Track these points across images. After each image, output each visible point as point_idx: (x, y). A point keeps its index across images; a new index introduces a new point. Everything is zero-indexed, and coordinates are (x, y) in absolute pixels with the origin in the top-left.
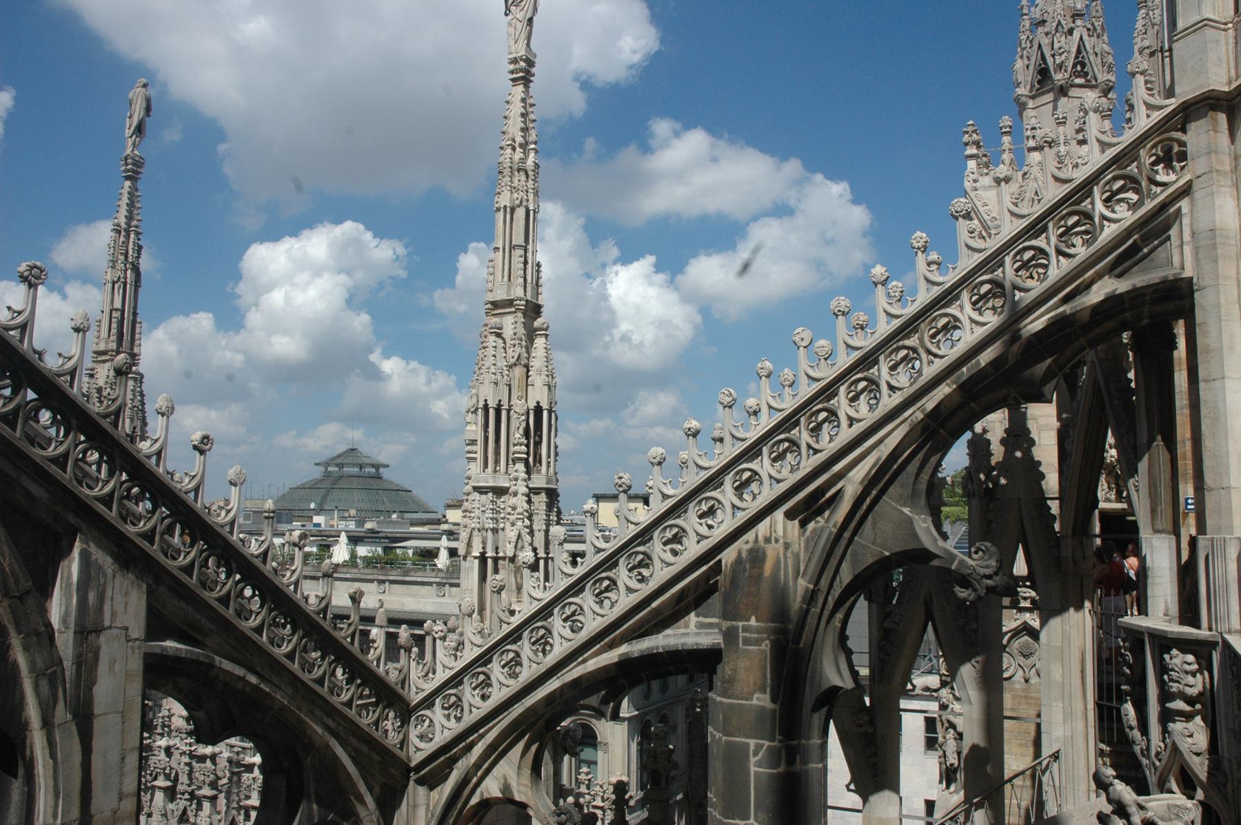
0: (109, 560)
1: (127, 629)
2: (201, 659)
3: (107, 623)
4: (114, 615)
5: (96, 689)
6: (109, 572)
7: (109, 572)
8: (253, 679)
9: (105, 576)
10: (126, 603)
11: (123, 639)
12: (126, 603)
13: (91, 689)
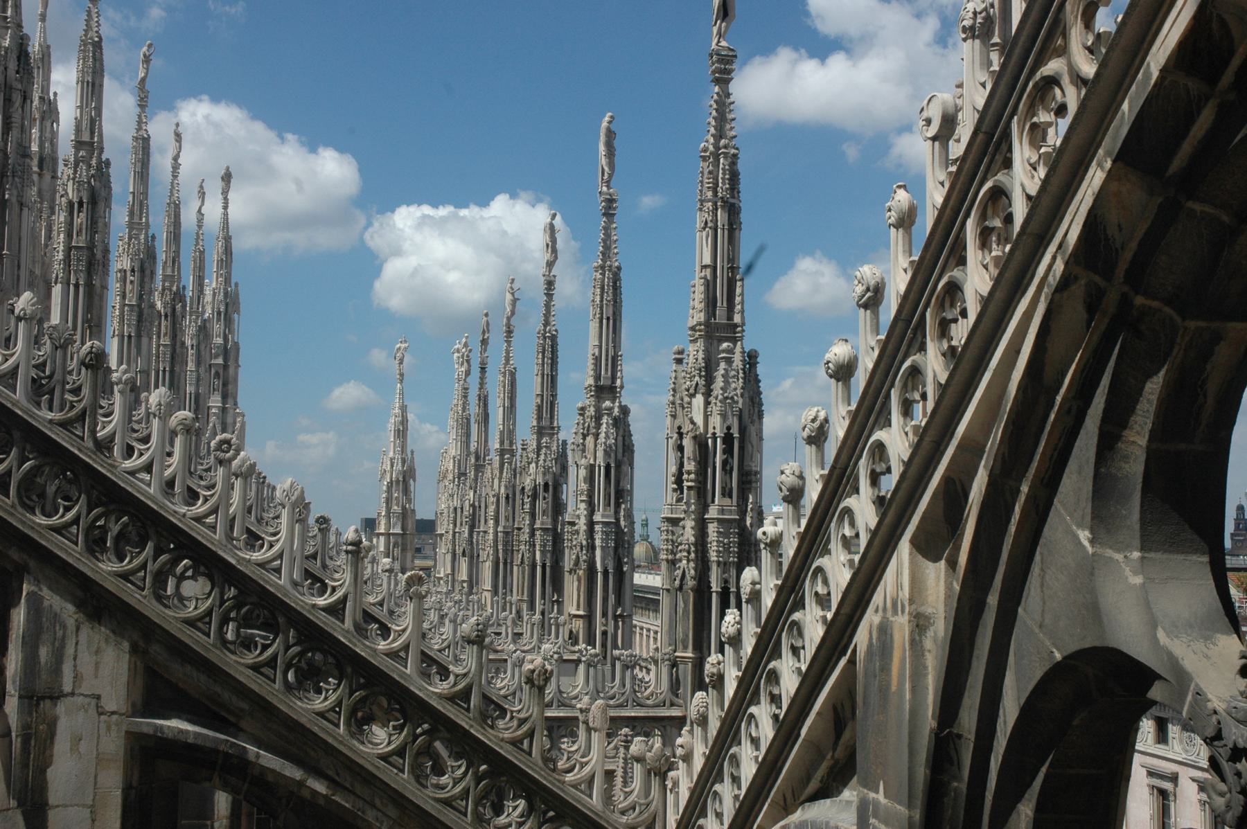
0: (70, 608)
1: (98, 697)
2: (222, 747)
3: (67, 688)
4: (77, 678)
5: (50, 773)
6: (71, 623)
7: (71, 623)
8: (320, 787)
9: (64, 627)
10: (97, 664)
11: (92, 711)
12: (97, 664)
13: (43, 771)
